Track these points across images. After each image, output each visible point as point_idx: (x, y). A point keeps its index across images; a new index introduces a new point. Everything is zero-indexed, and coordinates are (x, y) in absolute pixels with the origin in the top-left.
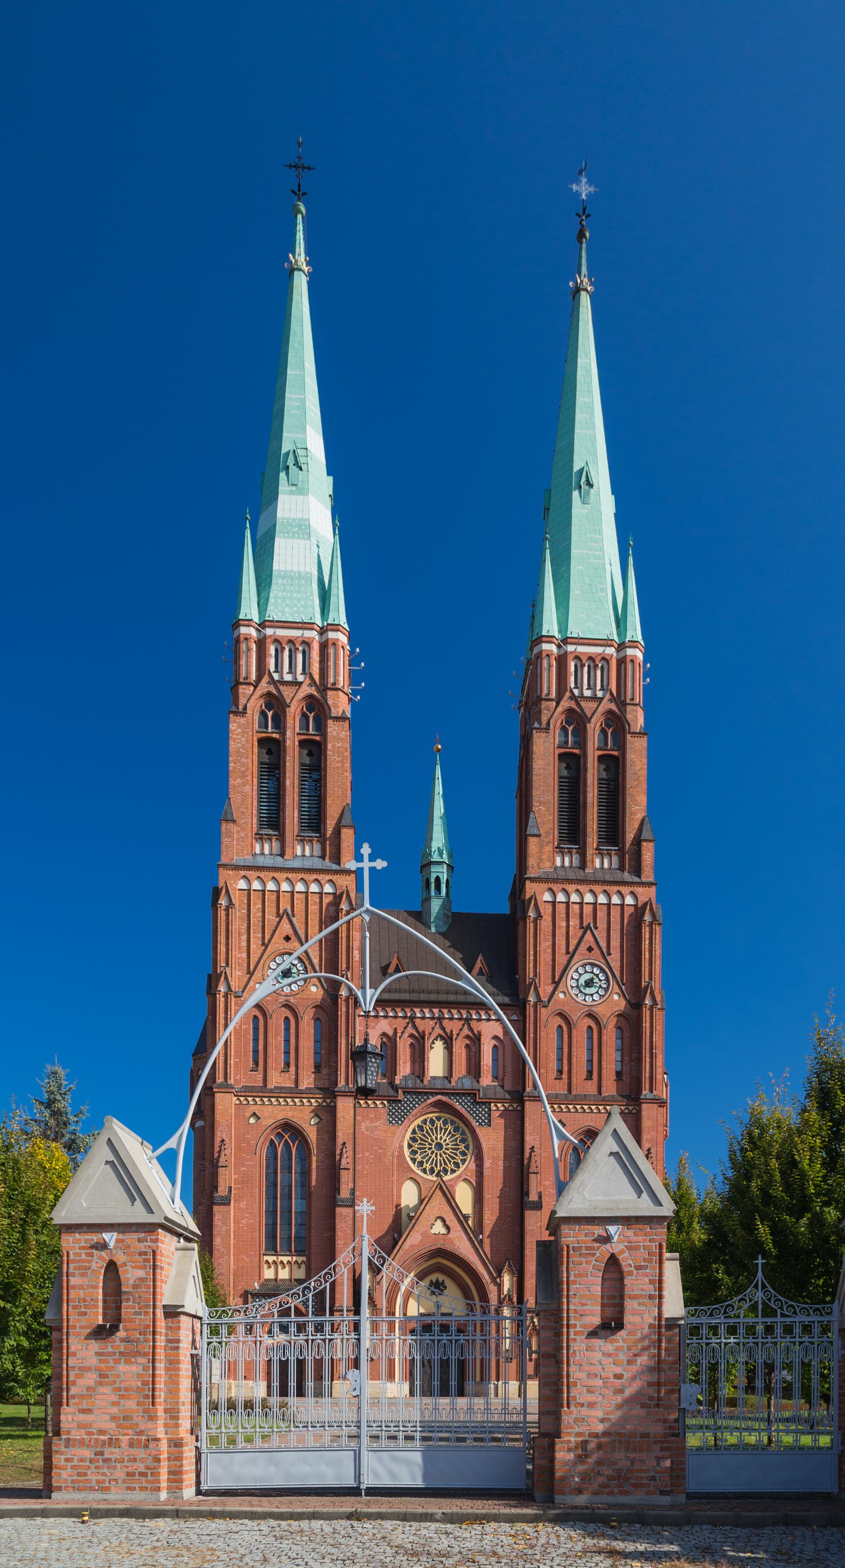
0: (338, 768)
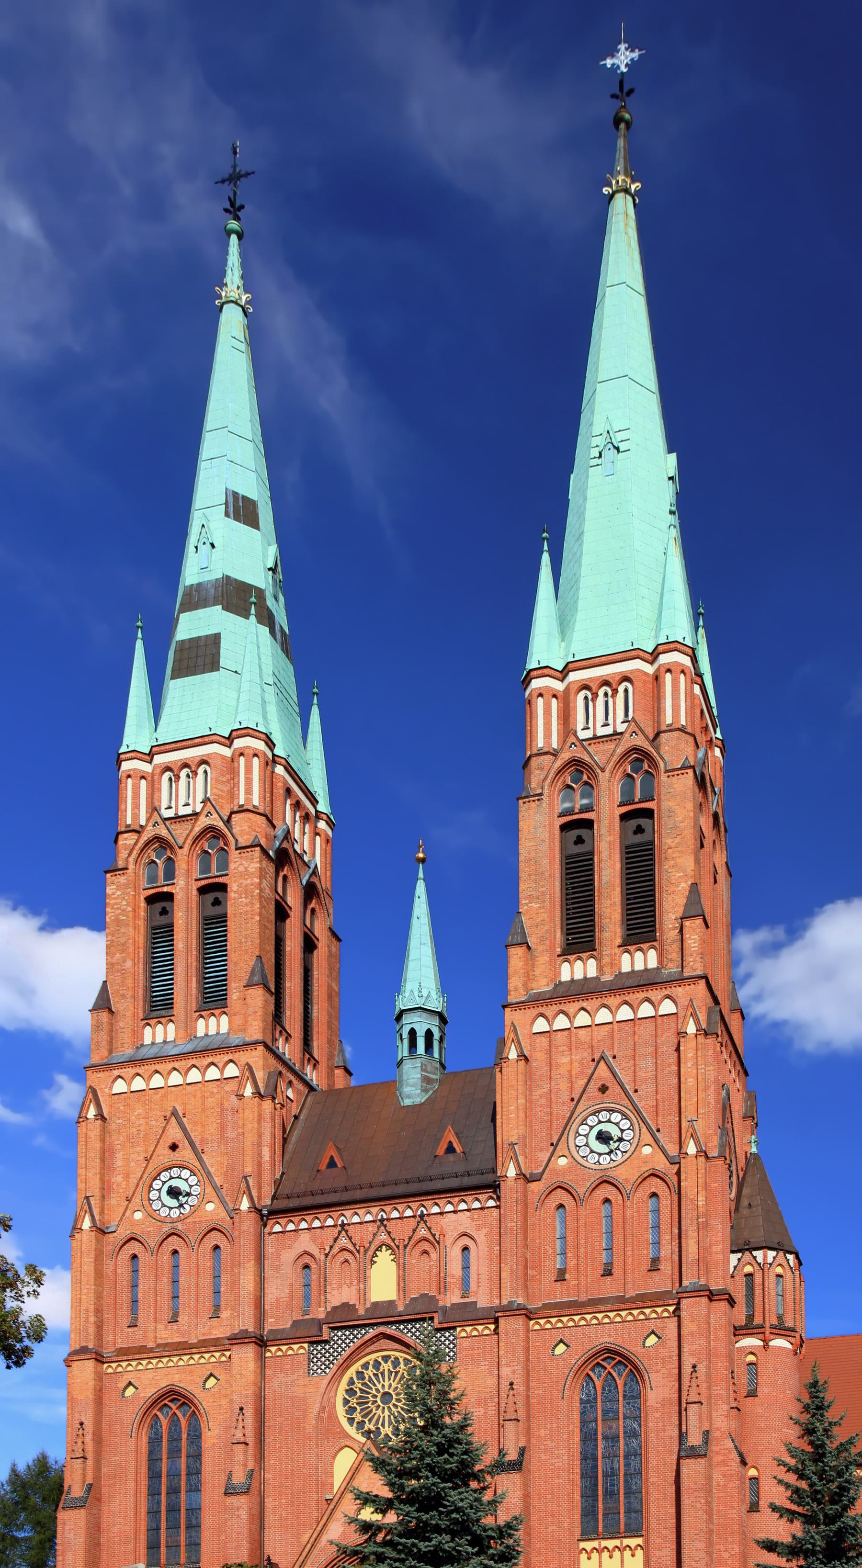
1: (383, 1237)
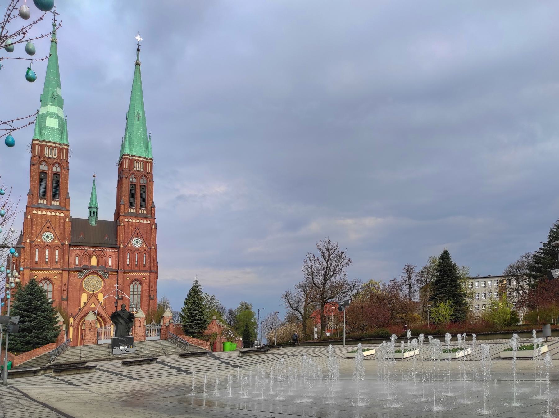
0: (65, 182)
1: (94, 253)
